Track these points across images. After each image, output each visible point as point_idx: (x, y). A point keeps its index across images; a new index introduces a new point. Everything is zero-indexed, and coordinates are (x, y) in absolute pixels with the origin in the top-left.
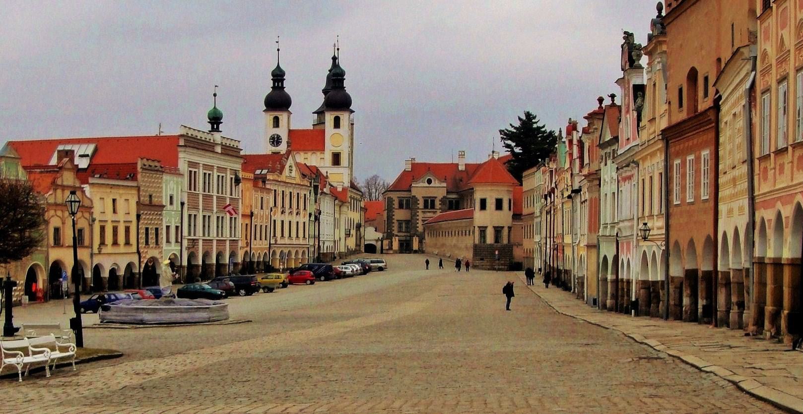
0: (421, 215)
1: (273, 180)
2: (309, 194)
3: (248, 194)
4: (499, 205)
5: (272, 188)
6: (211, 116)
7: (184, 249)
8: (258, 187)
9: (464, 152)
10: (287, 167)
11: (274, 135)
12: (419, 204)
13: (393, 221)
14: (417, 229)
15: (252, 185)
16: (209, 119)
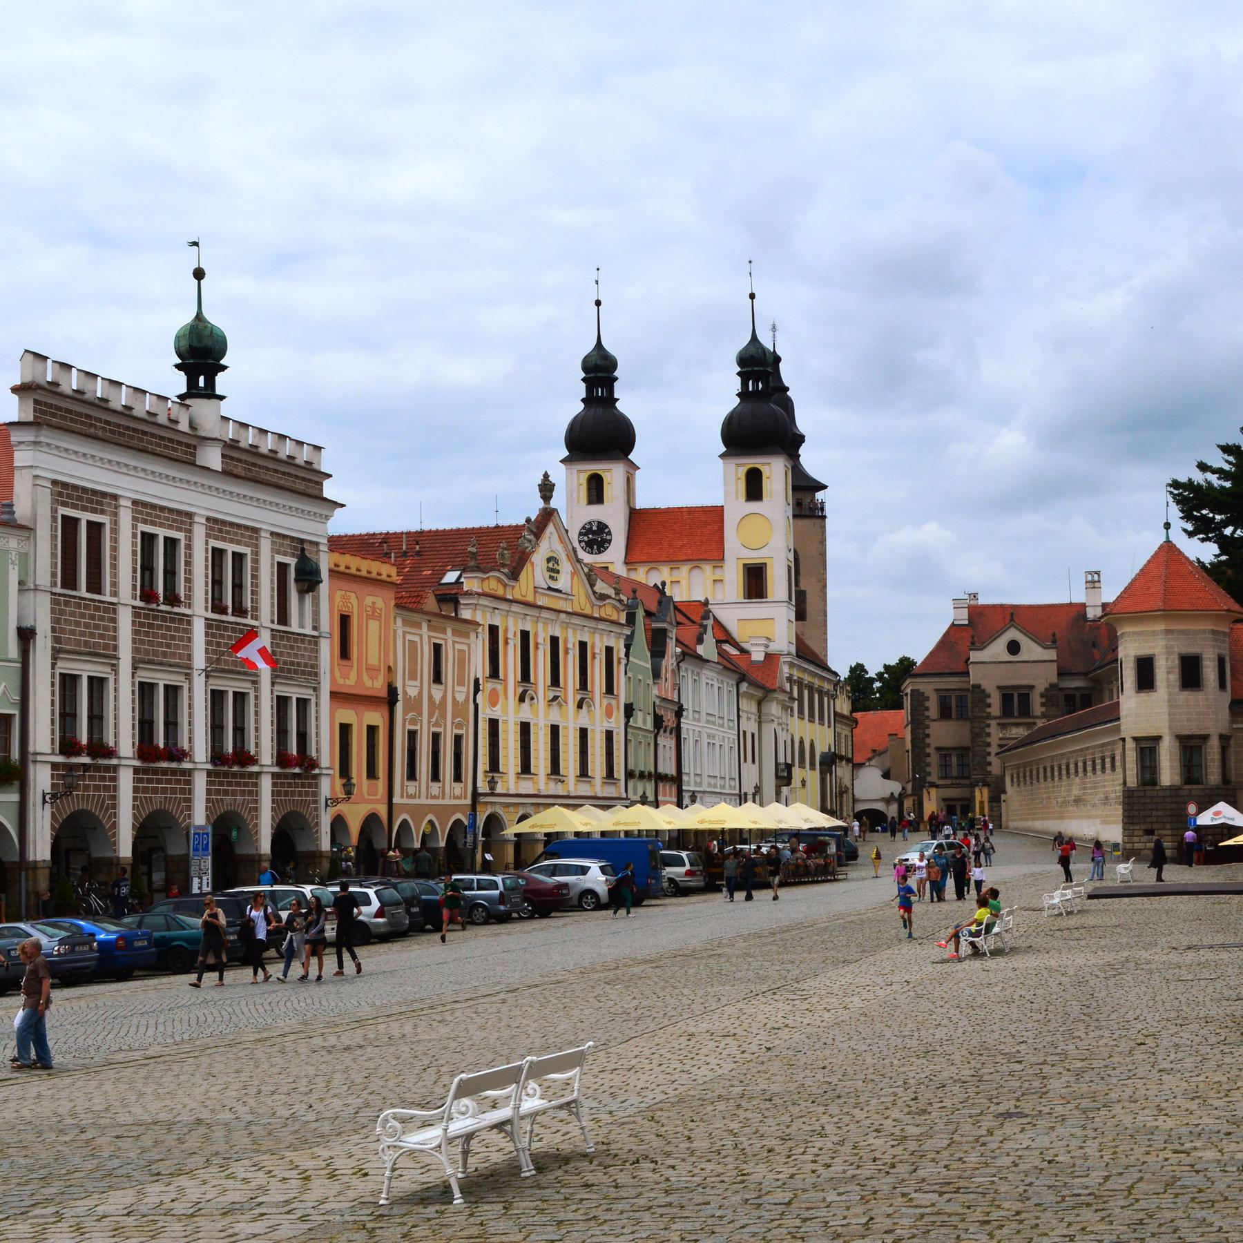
0: (995, 734)
1: (479, 594)
2: (623, 650)
3: (373, 626)
4: (1190, 672)
5: (479, 619)
6: (184, 344)
7: (35, 798)
8: (423, 612)
9: (1098, 573)
10: (538, 559)
11: (590, 523)
12: (989, 705)
13: (928, 750)
14: (989, 768)
15: (393, 603)
16: (179, 355)
